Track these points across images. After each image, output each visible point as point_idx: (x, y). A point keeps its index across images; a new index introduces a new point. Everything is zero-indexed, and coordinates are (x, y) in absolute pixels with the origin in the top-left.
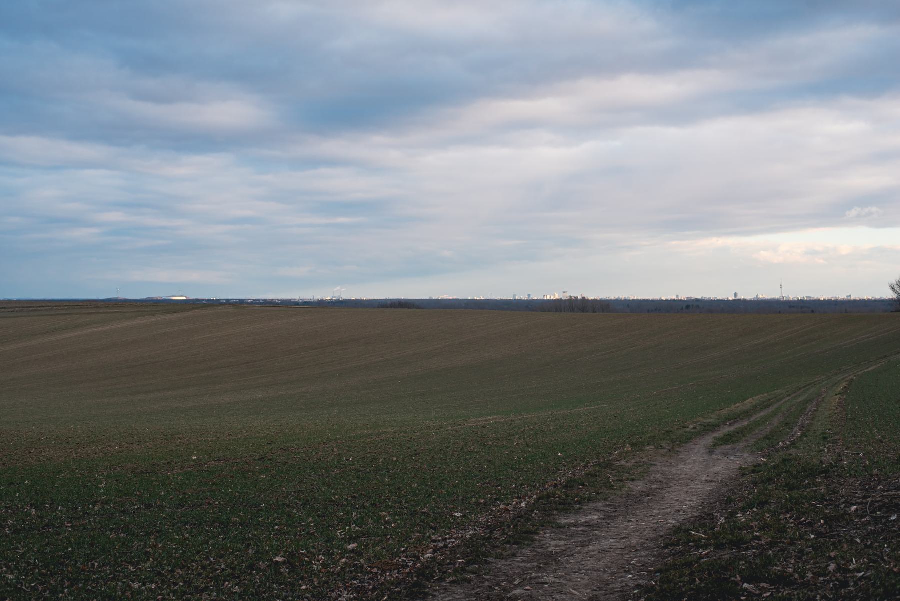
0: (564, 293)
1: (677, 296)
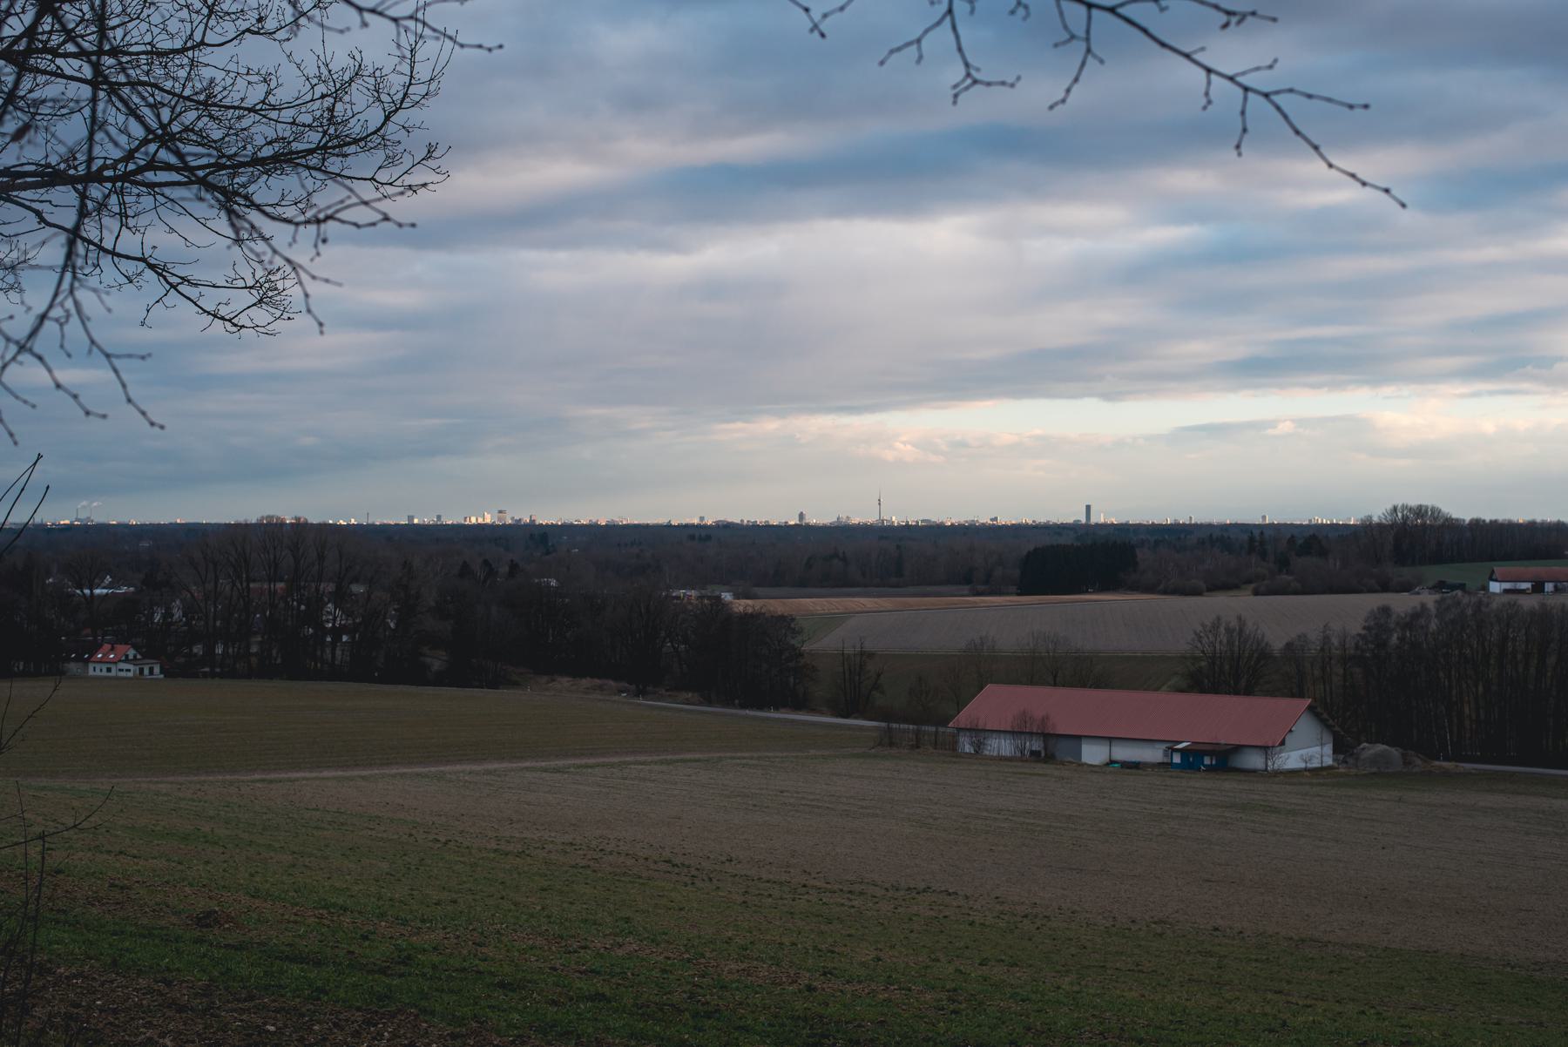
0: (500, 512)
1: (702, 518)
